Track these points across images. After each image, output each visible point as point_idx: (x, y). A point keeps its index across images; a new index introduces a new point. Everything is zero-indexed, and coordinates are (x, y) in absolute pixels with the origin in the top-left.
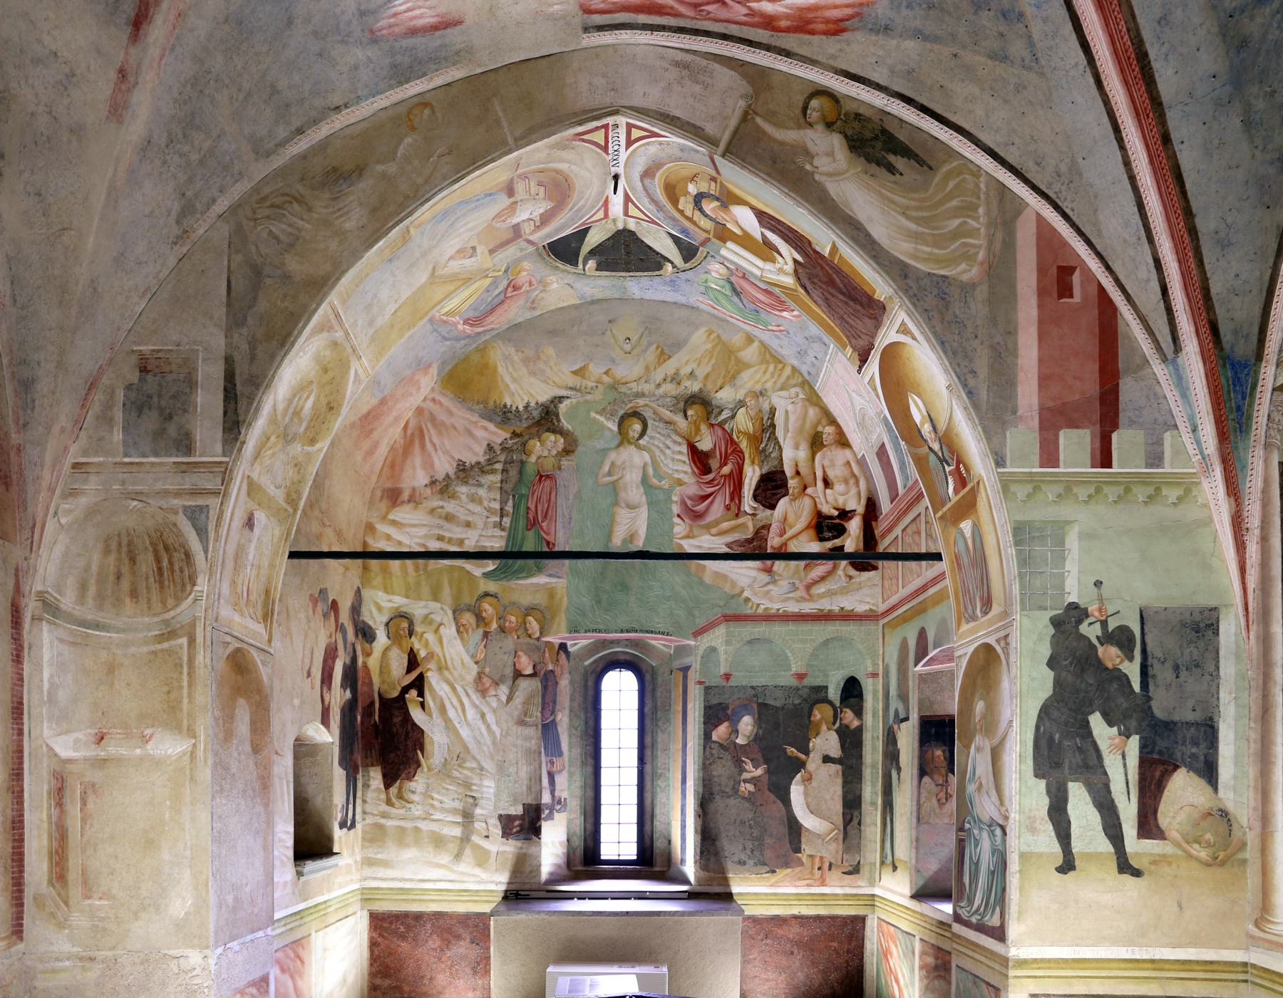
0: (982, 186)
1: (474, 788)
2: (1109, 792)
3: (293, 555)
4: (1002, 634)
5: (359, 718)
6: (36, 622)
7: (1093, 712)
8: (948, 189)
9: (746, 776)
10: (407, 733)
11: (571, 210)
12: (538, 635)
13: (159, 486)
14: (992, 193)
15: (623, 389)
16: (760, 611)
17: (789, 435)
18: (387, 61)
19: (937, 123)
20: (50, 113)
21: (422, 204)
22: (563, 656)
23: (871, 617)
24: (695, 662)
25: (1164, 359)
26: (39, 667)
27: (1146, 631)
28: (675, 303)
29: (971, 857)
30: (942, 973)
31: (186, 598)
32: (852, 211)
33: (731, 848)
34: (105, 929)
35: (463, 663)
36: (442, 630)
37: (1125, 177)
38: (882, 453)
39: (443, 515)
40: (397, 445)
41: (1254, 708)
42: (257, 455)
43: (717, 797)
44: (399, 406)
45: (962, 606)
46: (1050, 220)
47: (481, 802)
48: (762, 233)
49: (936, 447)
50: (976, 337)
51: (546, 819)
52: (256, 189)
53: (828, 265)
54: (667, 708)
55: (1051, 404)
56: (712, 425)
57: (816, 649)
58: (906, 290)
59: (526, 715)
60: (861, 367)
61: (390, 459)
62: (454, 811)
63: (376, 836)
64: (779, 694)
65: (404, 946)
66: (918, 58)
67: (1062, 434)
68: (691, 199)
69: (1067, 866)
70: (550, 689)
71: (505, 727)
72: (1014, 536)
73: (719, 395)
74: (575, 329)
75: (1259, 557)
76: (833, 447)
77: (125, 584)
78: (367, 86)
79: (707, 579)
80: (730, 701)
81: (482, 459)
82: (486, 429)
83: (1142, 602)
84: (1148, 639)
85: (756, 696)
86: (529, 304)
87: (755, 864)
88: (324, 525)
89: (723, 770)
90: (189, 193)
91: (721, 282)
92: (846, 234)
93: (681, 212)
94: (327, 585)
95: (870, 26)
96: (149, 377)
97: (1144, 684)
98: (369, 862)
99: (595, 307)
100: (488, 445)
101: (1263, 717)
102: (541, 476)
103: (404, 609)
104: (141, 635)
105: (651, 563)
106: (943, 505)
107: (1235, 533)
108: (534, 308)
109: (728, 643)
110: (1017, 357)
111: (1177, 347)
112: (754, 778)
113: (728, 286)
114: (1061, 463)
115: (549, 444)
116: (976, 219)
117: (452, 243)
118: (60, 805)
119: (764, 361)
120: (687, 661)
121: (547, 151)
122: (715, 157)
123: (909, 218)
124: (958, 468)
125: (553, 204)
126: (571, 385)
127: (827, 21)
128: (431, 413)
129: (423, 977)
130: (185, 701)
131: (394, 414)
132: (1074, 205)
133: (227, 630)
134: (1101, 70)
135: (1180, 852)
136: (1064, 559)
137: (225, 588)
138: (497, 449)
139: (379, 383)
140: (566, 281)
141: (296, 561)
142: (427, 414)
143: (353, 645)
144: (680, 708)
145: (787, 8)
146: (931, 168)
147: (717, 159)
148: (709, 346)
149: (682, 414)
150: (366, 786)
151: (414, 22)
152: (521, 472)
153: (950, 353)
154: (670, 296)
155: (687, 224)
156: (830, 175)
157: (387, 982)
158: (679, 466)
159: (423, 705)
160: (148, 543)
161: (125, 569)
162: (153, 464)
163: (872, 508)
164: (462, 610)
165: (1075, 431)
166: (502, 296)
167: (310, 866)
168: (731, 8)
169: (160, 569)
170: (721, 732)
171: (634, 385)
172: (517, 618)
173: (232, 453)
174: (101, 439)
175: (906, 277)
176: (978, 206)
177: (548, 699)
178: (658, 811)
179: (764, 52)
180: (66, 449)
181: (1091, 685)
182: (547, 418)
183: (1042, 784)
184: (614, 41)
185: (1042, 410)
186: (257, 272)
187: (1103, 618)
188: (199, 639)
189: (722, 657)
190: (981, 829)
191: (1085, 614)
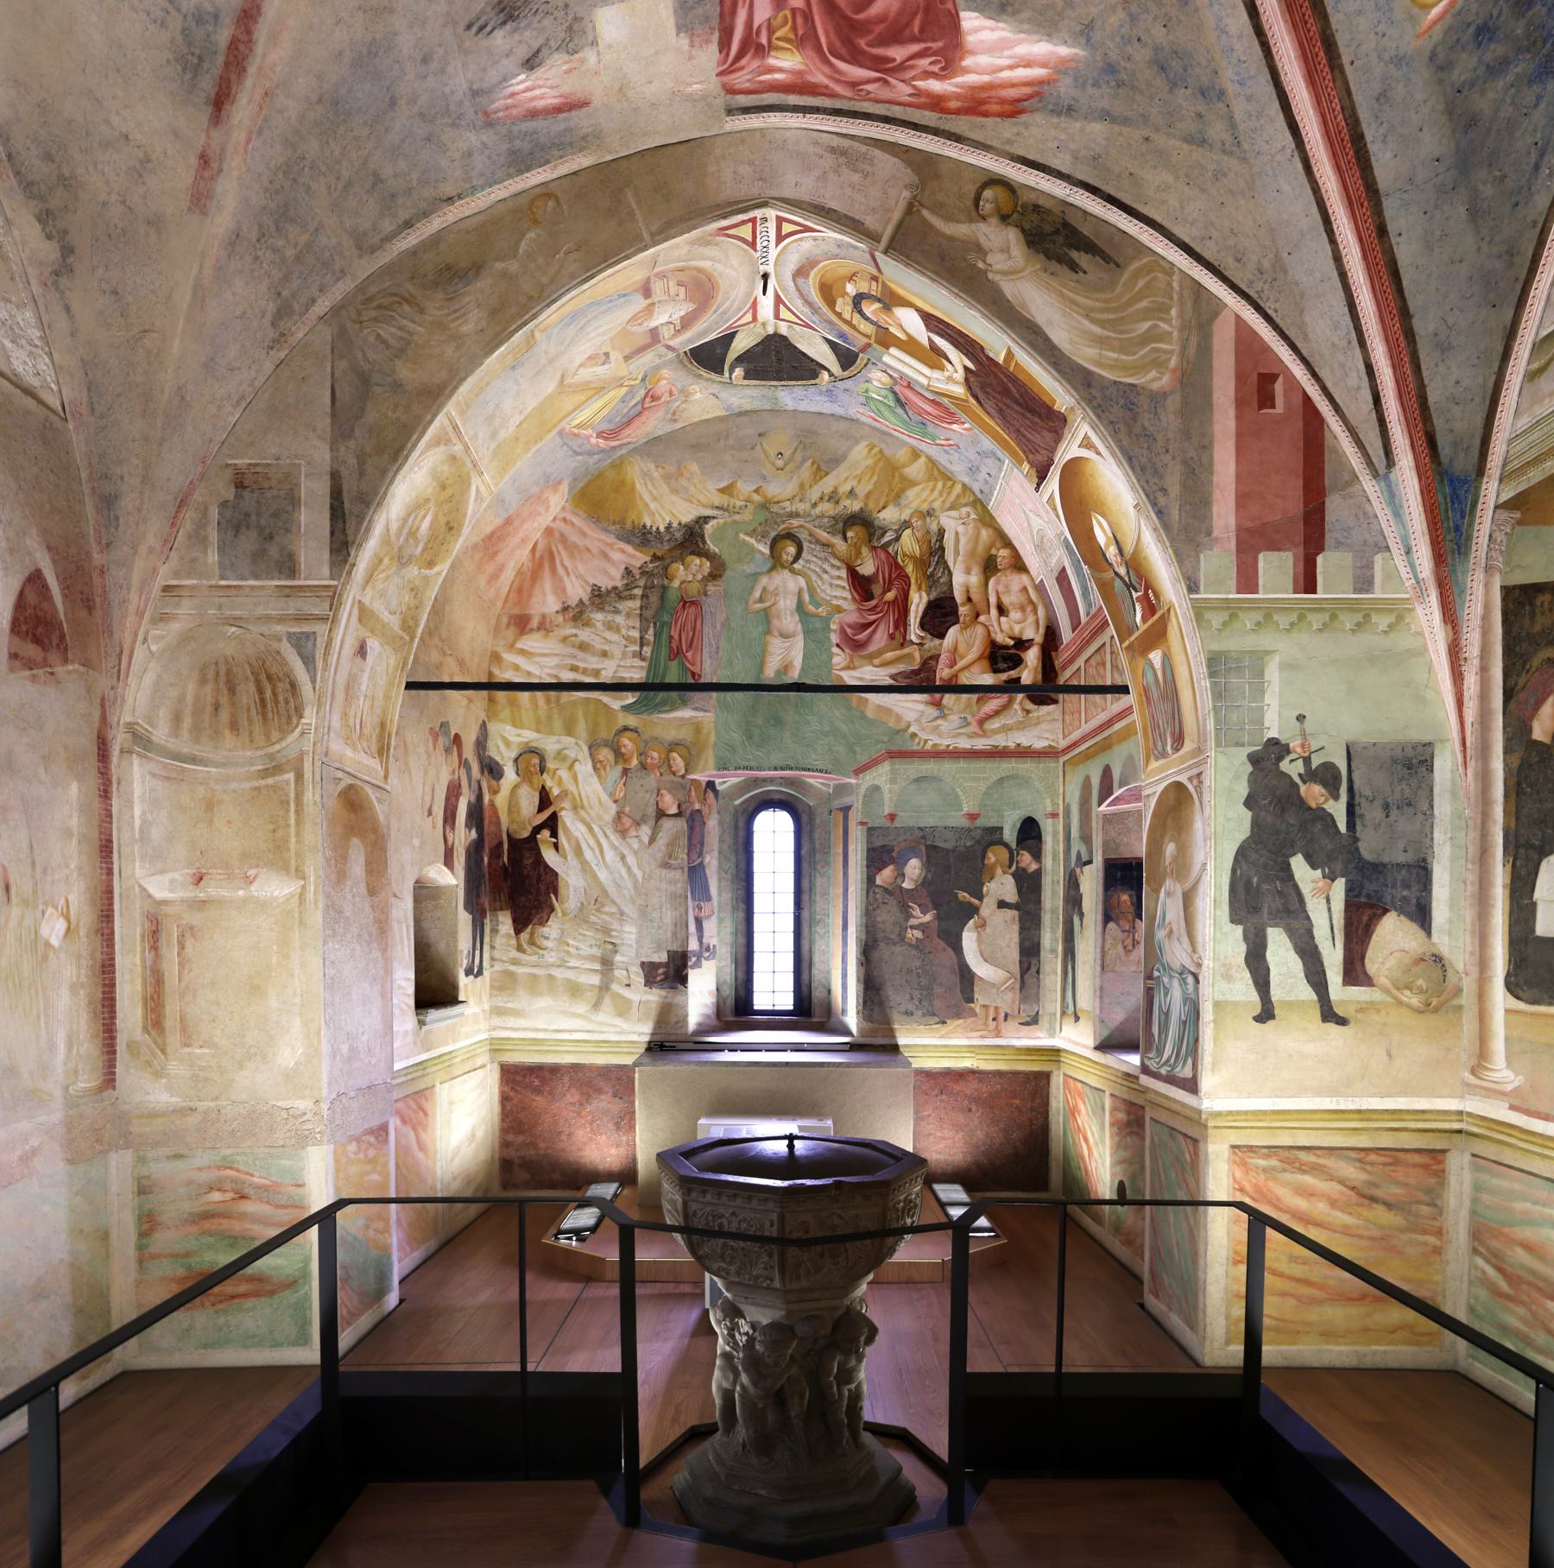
0: (1175, 285)
1: (614, 933)
2: (1313, 938)
3: (410, 686)
4: (1195, 771)
5: (486, 859)
6: (125, 755)
7: (1295, 854)
8: (1137, 289)
9: (913, 922)
10: (539, 876)
11: (715, 312)
12: (683, 772)
13: (260, 611)
14: (1186, 293)
15: (775, 509)
16: (928, 746)
17: (960, 558)
18: (505, 147)
19: (1125, 215)
20: (124, 202)
21: (548, 306)
22: (710, 794)
23: (1050, 753)
24: (857, 802)
25: (1375, 474)
26: (130, 804)
27: (1353, 768)
28: (832, 415)
29: (1160, 1006)
30: (1135, 1129)
31: (293, 731)
32: (1029, 313)
33: (896, 997)
34: (206, 1079)
35: (600, 802)
36: (577, 766)
37: (1335, 274)
38: (1062, 578)
39: (577, 644)
40: (525, 569)
41: (1471, 850)
42: (369, 579)
43: (882, 944)
44: (525, 526)
45: (1151, 742)
46: (1250, 323)
47: (621, 949)
48: (929, 339)
49: (1122, 571)
50: (1167, 451)
51: (693, 967)
52: (361, 288)
53: (1003, 373)
54: (826, 851)
55: (1249, 524)
56: (874, 548)
57: (989, 788)
58: (1089, 401)
59: (670, 857)
60: (1039, 485)
61: (517, 583)
62: (592, 958)
63: (506, 983)
64: (949, 835)
65: (539, 1101)
66: (1104, 142)
67: (1261, 556)
68: (850, 301)
69: (1266, 1014)
70: (697, 829)
71: (647, 870)
72: (1209, 666)
73: (882, 515)
74: (722, 443)
75: (1478, 688)
76: (1008, 572)
77: (224, 716)
78: (482, 175)
79: (870, 714)
80: (895, 843)
81: (619, 584)
82: (623, 551)
83: (1350, 737)
84: (1355, 776)
85: (923, 837)
86: (669, 416)
87: (924, 1015)
88: (445, 654)
89: (887, 916)
90: (285, 293)
91: (884, 392)
92: (1023, 339)
93: (839, 315)
94: (450, 718)
95: (1051, 107)
96: (246, 494)
97: (1351, 825)
98: (498, 1011)
99: (745, 419)
100: (626, 568)
101: (1481, 858)
102: (685, 603)
103: (534, 744)
104: (242, 770)
105: (807, 695)
106: (1130, 634)
107: (1452, 663)
108: (675, 421)
109: (893, 781)
110: (1212, 473)
111: (1390, 460)
112: (921, 924)
113: (891, 396)
114: (1261, 589)
115: (694, 568)
116: (1168, 321)
117: (583, 348)
118: (155, 948)
119: (931, 478)
120: (847, 800)
121: (686, 248)
122: (877, 253)
123: (1093, 321)
124: (1146, 593)
125: (694, 306)
126: (717, 504)
127: (1003, 101)
128: (562, 534)
129: (560, 1133)
130: (293, 840)
131: (520, 535)
132: (1278, 305)
133: (338, 765)
134: (1310, 154)
135: (1389, 999)
136: (1263, 692)
137: (336, 722)
138: (637, 573)
139: (503, 501)
140: (710, 391)
141: (414, 692)
142: (557, 535)
143: (479, 782)
144: (840, 851)
145: (957, 86)
146: (1118, 265)
147: (879, 255)
148: (870, 462)
149: (840, 535)
150: (494, 931)
152: (662, 598)
153: (1138, 470)
154: (827, 407)
155: (845, 328)
156: (1004, 273)
157: (520, 1138)
158: (836, 591)
159: (556, 846)
160: (249, 672)
161: (224, 700)
162: (252, 588)
163: (1051, 637)
164: (599, 746)
165: (1276, 553)
166: (639, 407)
167: (433, 1014)
168: (894, 87)
169: (262, 700)
170: (885, 876)
171: (787, 504)
172: (659, 753)
173: (340, 576)
174: (193, 560)
175: (1089, 385)
176: (1171, 307)
177: (694, 841)
178: (816, 958)
179: (931, 137)
180: (155, 570)
181: (1292, 826)
182: (691, 539)
183: (1239, 930)
184: (762, 125)
185: (1240, 531)
186: (364, 381)
187: (1307, 754)
188: (308, 775)
189: (887, 796)
190: (1171, 977)
191: (1286, 750)
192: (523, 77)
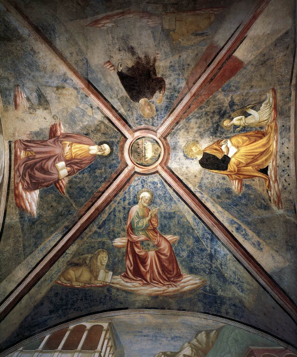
151: (18, 97)
192: (25, 96)
